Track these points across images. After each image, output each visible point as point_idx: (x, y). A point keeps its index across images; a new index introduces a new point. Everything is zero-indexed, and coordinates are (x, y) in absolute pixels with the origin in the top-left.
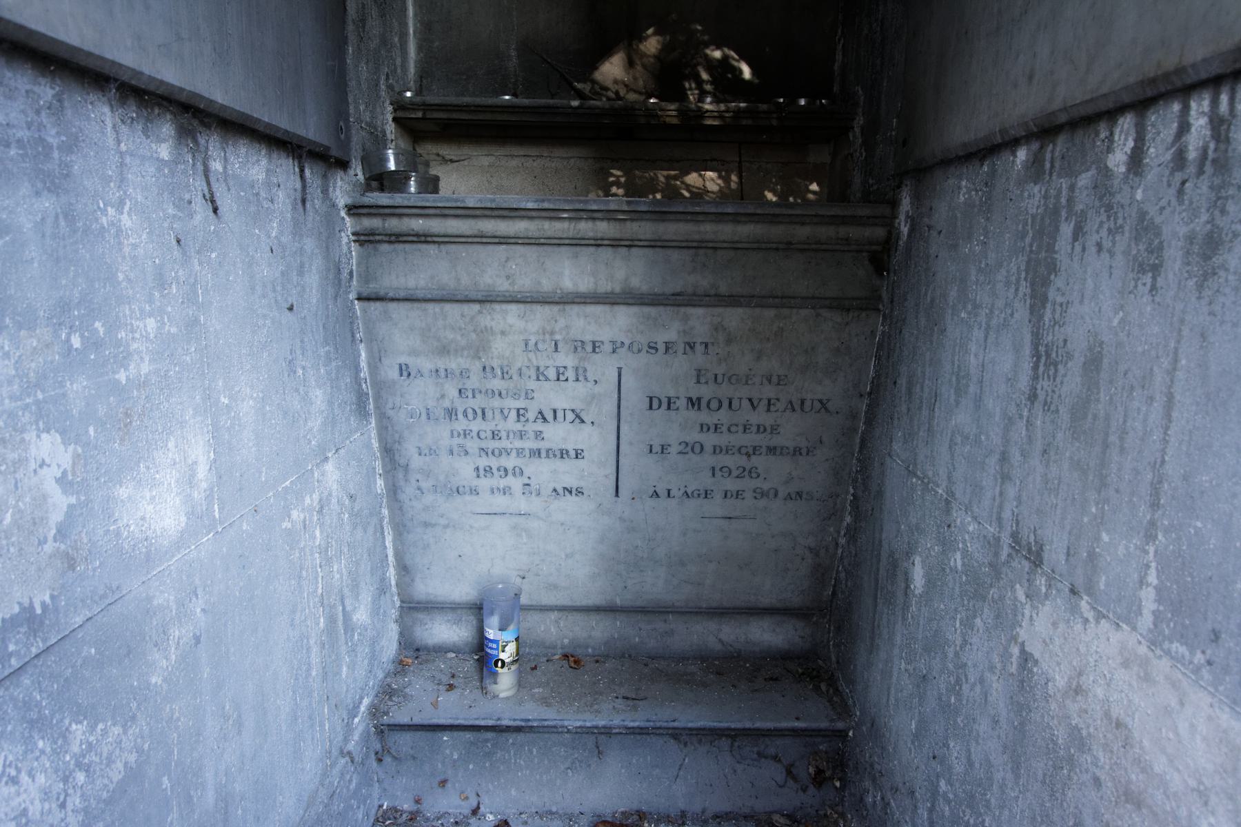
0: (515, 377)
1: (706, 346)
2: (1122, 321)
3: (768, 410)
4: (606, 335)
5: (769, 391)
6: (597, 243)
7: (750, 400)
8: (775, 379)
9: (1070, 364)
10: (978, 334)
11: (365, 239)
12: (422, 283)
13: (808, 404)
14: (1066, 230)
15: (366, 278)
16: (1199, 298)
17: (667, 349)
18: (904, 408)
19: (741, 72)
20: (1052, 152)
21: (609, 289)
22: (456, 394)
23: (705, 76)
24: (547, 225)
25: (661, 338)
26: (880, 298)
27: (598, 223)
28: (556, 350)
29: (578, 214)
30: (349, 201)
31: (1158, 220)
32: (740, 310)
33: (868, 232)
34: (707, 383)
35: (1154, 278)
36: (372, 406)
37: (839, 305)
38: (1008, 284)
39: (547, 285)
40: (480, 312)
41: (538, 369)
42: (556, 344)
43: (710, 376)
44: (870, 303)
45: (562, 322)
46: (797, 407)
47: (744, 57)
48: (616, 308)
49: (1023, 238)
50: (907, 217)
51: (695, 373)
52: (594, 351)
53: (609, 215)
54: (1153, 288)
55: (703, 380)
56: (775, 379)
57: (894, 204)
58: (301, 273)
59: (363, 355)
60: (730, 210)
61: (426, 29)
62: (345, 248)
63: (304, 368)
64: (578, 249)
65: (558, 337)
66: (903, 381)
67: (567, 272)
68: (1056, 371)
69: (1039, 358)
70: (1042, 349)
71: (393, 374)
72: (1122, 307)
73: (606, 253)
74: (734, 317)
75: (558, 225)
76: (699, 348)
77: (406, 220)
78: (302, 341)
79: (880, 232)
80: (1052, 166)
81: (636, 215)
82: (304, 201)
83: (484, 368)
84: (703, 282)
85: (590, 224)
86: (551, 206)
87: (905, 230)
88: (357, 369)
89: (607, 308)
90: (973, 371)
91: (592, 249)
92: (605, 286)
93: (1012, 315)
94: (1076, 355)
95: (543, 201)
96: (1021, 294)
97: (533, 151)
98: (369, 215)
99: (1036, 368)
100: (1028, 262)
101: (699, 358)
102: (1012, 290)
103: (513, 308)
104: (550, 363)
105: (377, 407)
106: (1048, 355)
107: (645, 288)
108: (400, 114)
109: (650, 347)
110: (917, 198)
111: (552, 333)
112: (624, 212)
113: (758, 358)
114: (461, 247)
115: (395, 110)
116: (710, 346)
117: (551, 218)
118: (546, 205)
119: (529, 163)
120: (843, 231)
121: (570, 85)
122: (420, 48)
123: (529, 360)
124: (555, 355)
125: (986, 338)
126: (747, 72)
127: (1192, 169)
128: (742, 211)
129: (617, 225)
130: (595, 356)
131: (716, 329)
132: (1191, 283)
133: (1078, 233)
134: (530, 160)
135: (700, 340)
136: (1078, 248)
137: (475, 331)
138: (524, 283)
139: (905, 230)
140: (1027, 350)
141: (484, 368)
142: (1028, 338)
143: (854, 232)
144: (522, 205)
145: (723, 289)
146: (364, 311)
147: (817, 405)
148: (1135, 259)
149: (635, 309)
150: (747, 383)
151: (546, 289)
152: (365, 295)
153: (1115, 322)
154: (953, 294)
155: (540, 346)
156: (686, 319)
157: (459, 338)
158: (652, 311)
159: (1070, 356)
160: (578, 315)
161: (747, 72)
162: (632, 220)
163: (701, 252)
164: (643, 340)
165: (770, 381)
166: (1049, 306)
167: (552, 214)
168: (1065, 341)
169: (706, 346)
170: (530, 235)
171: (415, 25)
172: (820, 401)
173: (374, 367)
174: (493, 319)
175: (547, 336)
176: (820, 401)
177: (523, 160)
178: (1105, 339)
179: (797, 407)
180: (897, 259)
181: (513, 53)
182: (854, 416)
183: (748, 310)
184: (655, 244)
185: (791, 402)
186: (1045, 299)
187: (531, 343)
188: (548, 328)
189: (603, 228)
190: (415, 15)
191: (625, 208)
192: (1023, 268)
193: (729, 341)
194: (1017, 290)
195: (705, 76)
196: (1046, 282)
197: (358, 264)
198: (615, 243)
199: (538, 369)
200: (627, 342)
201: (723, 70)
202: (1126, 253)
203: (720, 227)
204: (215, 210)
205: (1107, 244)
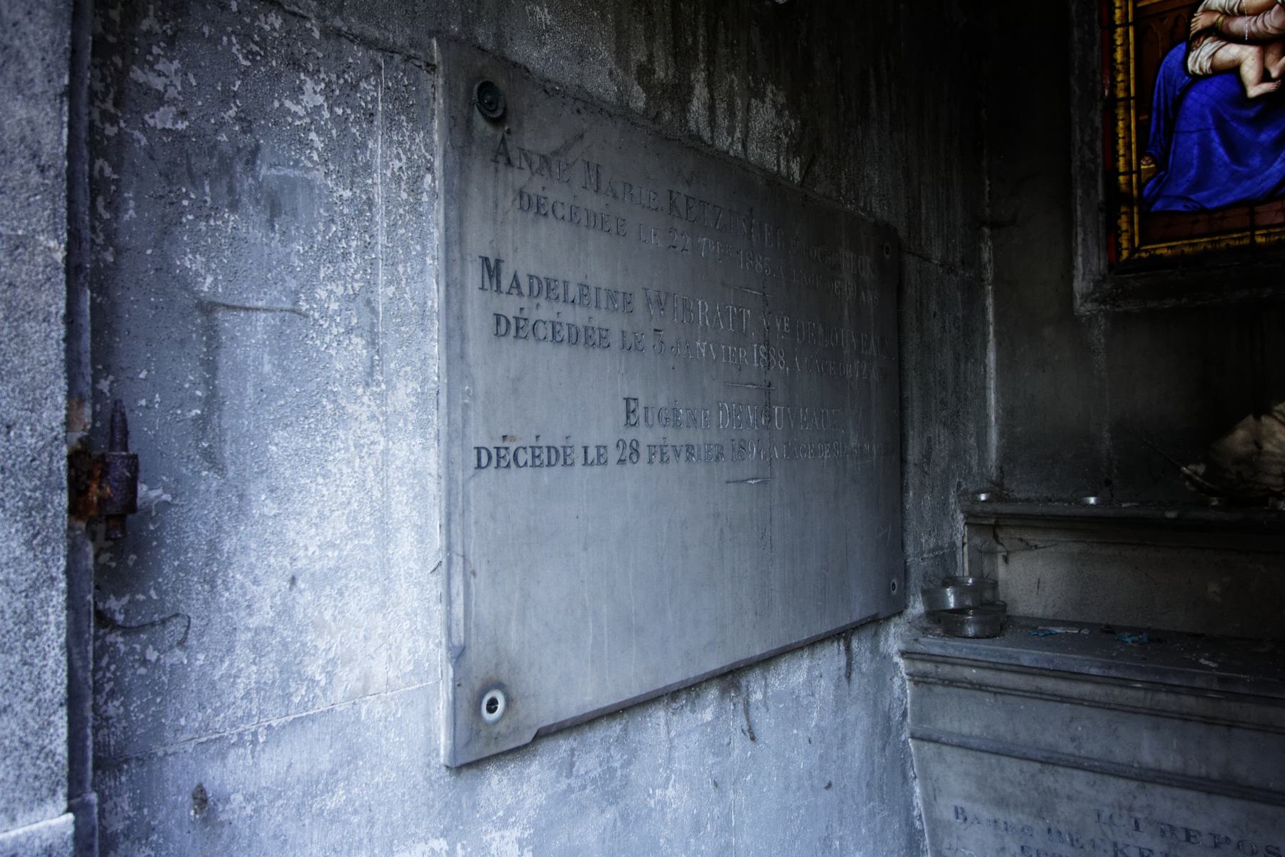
0: (1088, 848)
6: (1185, 717)
11: (920, 680)
12: (976, 731)
15: (920, 718)
21: (1203, 771)
22: (1018, 851)
24: (1117, 691)
28: (1137, 828)
29: (1153, 687)
30: (903, 647)
36: (927, 841)
39: (1120, 754)
40: (1042, 772)
41: (1115, 845)
42: (1136, 822)
45: (1141, 801)
58: (842, 745)
59: (918, 790)
61: (1009, 414)
62: (897, 691)
63: (841, 838)
65: (1138, 815)
71: (949, 815)
75: (1130, 693)
77: (959, 669)
78: (841, 812)
82: (848, 676)
83: (1049, 830)
85: (1172, 698)
88: (909, 807)
92: (1197, 768)
95: (1110, 668)
98: (922, 660)
104: (1130, 841)
105: (932, 844)
108: (971, 520)
114: (1019, 700)
115: (966, 518)
117: (1120, 686)
118: (1113, 673)
122: (1001, 435)
123: (1104, 834)
124: (1137, 834)
137: (1036, 789)
141: (1049, 830)
144: (1085, 670)
146: (917, 748)
152: (917, 735)
155: (1116, 820)
157: (1018, 793)
158: (1269, 810)
170: (1097, 698)
171: (997, 412)
173: (929, 805)
174: (1057, 781)
175: (1125, 812)
181: (1106, 435)
189: (1189, 702)
190: (997, 402)
191: (1216, 686)
197: (913, 703)
199: (1115, 845)
200: (1235, 839)
204: (753, 739)
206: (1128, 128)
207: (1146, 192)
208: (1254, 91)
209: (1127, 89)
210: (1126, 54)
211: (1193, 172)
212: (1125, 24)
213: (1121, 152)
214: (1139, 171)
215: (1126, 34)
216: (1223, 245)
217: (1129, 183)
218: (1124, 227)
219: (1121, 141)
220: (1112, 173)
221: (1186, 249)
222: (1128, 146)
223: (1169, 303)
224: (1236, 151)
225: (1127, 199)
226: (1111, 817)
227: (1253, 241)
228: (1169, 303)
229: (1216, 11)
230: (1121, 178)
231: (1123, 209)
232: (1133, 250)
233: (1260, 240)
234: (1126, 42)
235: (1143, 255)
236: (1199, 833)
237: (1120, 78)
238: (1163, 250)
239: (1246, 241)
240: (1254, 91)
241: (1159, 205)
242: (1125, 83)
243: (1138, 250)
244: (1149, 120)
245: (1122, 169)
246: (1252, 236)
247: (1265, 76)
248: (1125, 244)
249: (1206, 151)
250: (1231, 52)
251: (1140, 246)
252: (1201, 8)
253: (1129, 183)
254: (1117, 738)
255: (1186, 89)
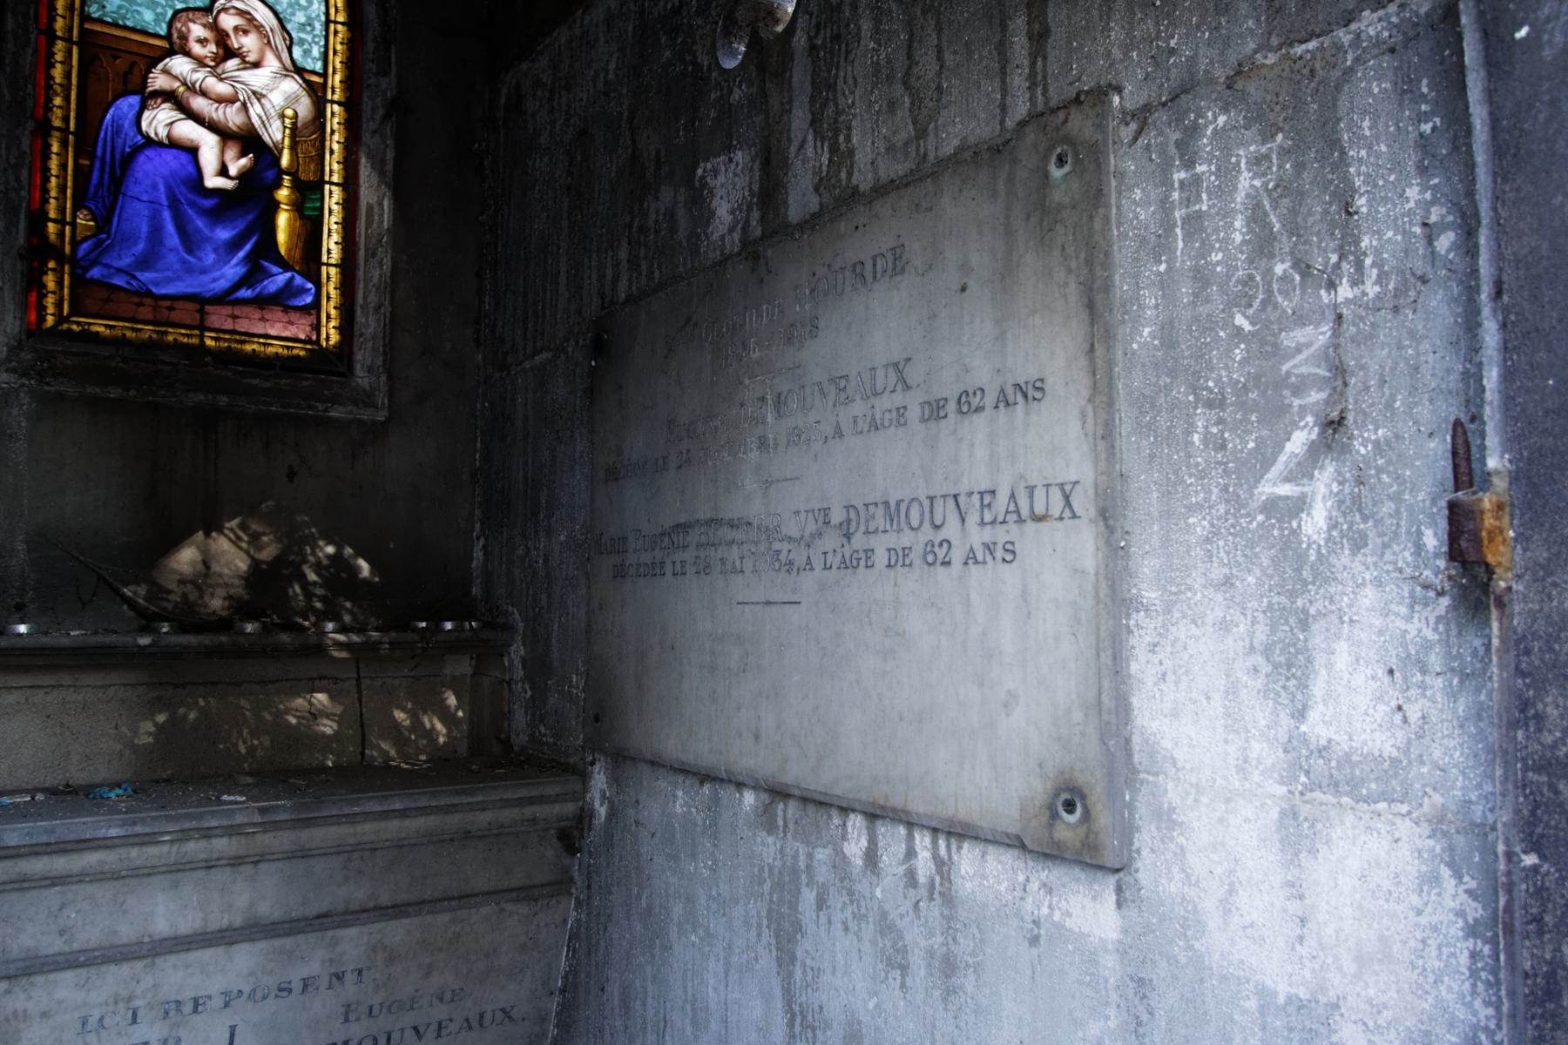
1: (360, 972)
2: (877, 1006)
3: (439, 1036)
4: (214, 986)
5: (441, 1012)
7: (415, 1028)
8: (448, 996)
9: (829, 1033)
10: (714, 967)
13: (488, 1017)
14: (808, 897)
16: (945, 1009)
17: (305, 987)
18: (619, 1023)
19: (358, 569)
20: (785, 811)
21: (225, 923)
23: (312, 577)
24: (134, 852)
25: (296, 976)
26: (571, 879)
27: (214, 841)
28: (134, 1020)
31: (900, 924)
32: (406, 921)
33: (556, 809)
34: (358, 1019)
35: (903, 976)
37: (527, 893)
38: (747, 924)
39: (127, 933)
42: (135, 1015)
43: (364, 1009)
44: (561, 885)
45: (148, 981)
46: (475, 1024)
47: (360, 553)
48: (235, 947)
49: (761, 882)
50: (603, 796)
51: (343, 1010)
52: (195, 1011)
53: (232, 831)
54: (903, 986)
55: (352, 1017)
56: (448, 996)
57: (584, 777)
60: (398, 806)
64: (179, 875)
65: (138, 1003)
66: (614, 990)
67: (161, 910)
68: (815, 1036)
69: (793, 1016)
70: (797, 1009)
72: (876, 994)
73: (222, 876)
74: (397, 931)
75: (153, 851)
76: (350, 978)
79: (570, 808)
80: (786, 826)
81: (266, 827)
84: (358, 894)
85: (203, 844)
86: (148, 830)
87: (602, 811)
89: (220, 950)
90: (713, 1007)
91: (201, 873)
92: (219, 920)
93: (756, 959)
94: (835, 1026)
95: (134, 823)
96: (764, 942)
97: (46, 680)
99: (791, 1024)
100: (769, 911)
101: (350, 989)
102: (754, 932)
103: (69, 975)
106: (804, 1018)
107: (277, 914)
109: (280, 990)
110: (615, 780)
111: (130, 999)
112: (254, 824)
113: (428, 974)
116: (365, 973)
118: (139, 829)
119: (39, 697)
120: (528, 811)
121: (117, 592)
125: (726, 975)
126: (364, 566)
127: (923, 892)
128: (413, 805)
129: (243, 840)
130: (197, 1018)
131: (374, 950)
132: (937, 993)
133: (821, 903)
134: (41, 693)
135: (352, 967)
136: (823, 920)
138: (91, 935)
139: (602, 811)
140: (779, 1004)
142: (778, 991)
143: (540, 811)
144: (101, 833)
145: (385, 899)
147: (500, 1015)
148: (883, 951)
149: (263, 945)
150: (412, 1008)
151: (125, 940)
153: (871, 1005)
154: (678, 910)
155: (107, 1022)
156: (335, 943)
158: (288, 942)
159: (828, 1026)
160: (175, 967)
161: (364, 566)
162: (265, 832)
163: (356, 855)
164: (272, 982)
165: (441, 999)
166: (798, 964)
168: (821, 1008)
169: (360, 972)
172: (503, 1011)
176: (503, 1011)
177: (28, 692)
178: (864, 1020)
179: (475, 1024)
180: (593, 838)
181: (20, 547)
182: (543, 1020)
183: (416, 920)
185: (467, 1020)
186: (793, 959)
187: (93, 1021)
188: (125, 994)
189: (221, 845)
191: (258, 819)
192: (764, 914)
193: (390, 960)
194: (759, 935)
195: (312, 577)
196: (792, 940)
198: (236, 862)
200: (247, 989)
201: (339, 575)
202: (874, 943)
203: (384, 824)
205: (853, 926)
206: (63, 166)
207: (81, 253)
208: (212, 181)
209: (66, 119)
210: (67, 75)
211: (141, 246)
212: (68, 39)
213: (53, 193)
214: (73, 224)
215: (69, 53)
216: (170, 338)
217: (61, 234)
218: (51, 285)
219: (53, 180)
220: (38, 219)
221: (129, 334)
222: (62, 189)
223: (114, 393)
224: (190, 241)
225: (55, 252)
226: (101, 1019)
227: (202, 342)
228: (114, 393)
229: (176, 78)
230: (52, 227)
231: (51, 265)
232: (60, 318)
233: (209, 342)
234: (67, 61)
235: (74, 327)
236: (210, 997)
237: (58, 101)
238: (99, 327)
239: (195, 341)
240: (212, 181)
241: (95, 273)
242: (62, 110)
243: (66, 320)
244: (91, 167)
245: (52, 215)
246: (202, 337)
247: (223, 171)
248: (51, 310)
249: (156, 230)
250: (188, 130)
251: (71, 314)
252: (160, 66)
253: (61, 234)
254: (125, 912)
255: (138, 149)
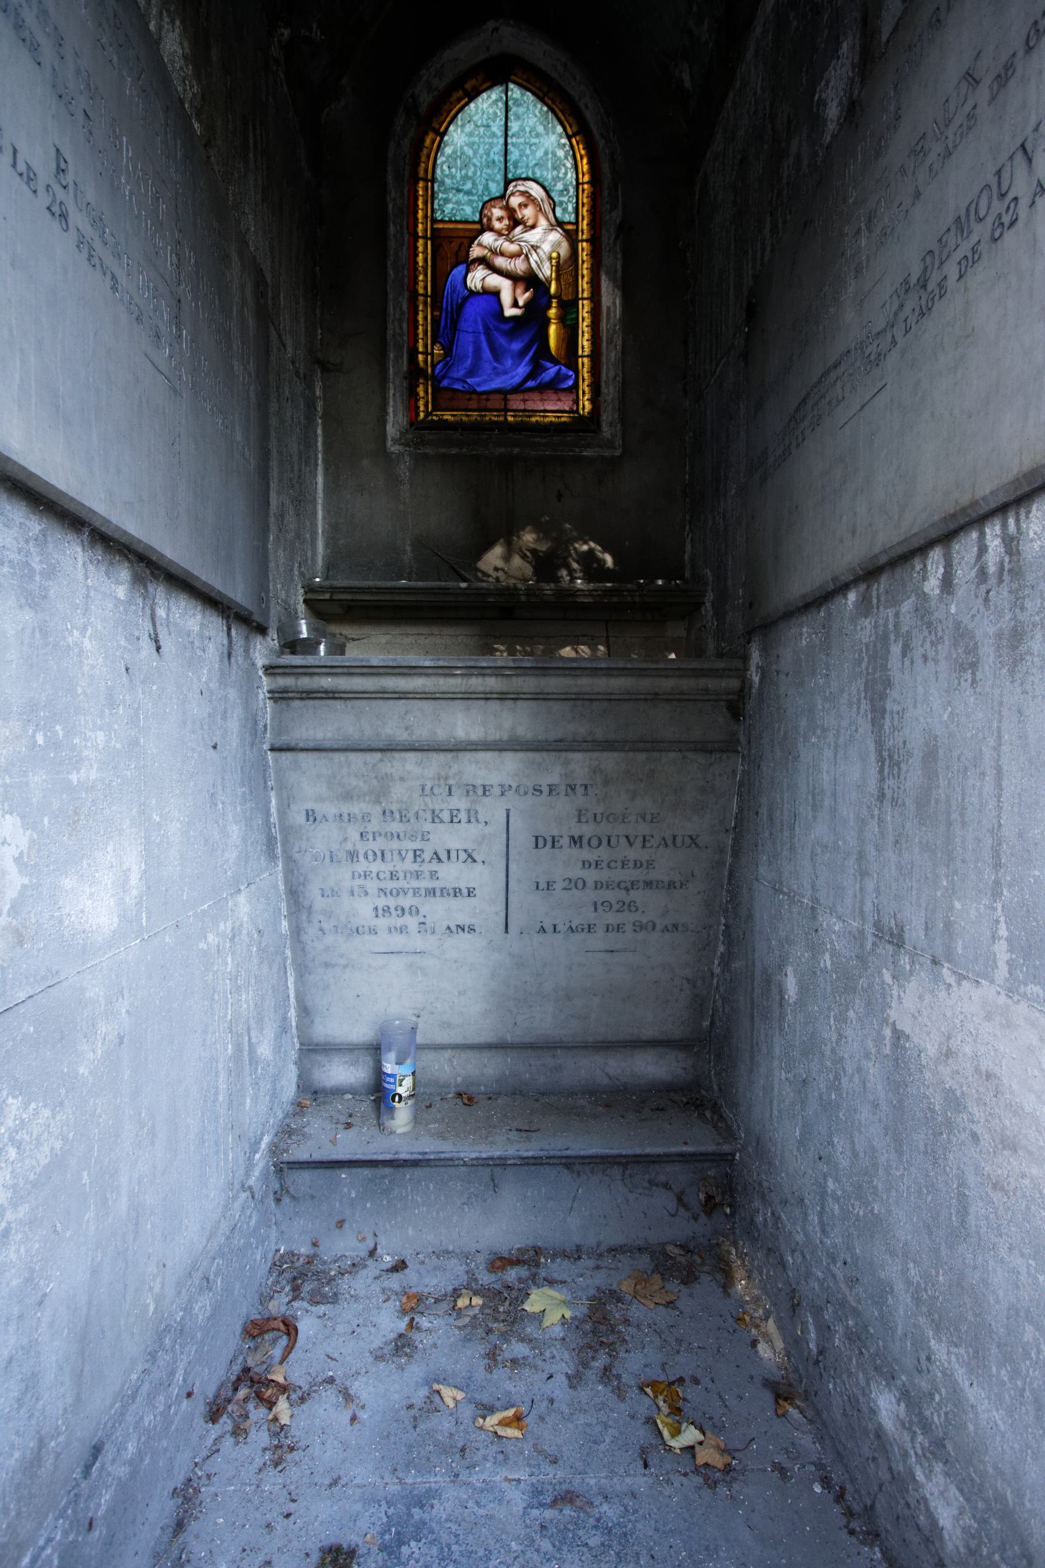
0: (413, 820)
3: (644, 846)
4: (494, 778)
5: (644, 829)
6: (487, 697)
7: (627, 837)
8: (648, 817)
9: (911, 761)
10: (828, 753)
11: (279, 696)
12: (329, 735)
13: (679, 840)
14: (896, 650)
15: (279, 731)
16: (1012, 682)
17: (551, 791)
18: (767, 834)
19: (605, 562)
20: (878, 590)
21: (498, 737)
22: (358, 837)
23: (575, 566)
24: (442, 681)
25: (545, 781)
26: (738, 741)
28: (450, 794)
29: (470, 671)
30: (267, 662)
31: (970, 626)
32: (615, 754)
34: (587, 822)
35: (973, 674)
36: (279, 851)
37: (703, 748)
39: (442, 735)
40: (382, 760)
41: (433, 812)
42: (450, 789)
43: (590, 815)
44: (729, 746)
46: (670, 843)
47: (605, 549)
49: (860, 664)
50: (758, 667)
51: (576, 813)
52: (484, 794)
53: (497, 671)
55: (583, 819)
56: (648, 817)
57: (745, 658)
58: (224, 718)
59: (273, 802)
61: (333, 529)
62: (261, 703)
63: (223, 803)
64: (470, 702)
65: (451, 782)
66: (764, 811)
67: (460, 723)
68: (899, 769)
69: (883, 763)
70: (885, 754)
71: (301, 819)
72: (949, 703)
73: (495, 705)
74: (610, 761)
75: (452, 681)
76: (580, 790)
77: (316, 679)
78: (223, 779)
79: (734, 684)
80: (879, 600)
82: (229, 655)
83: (384, 812)
84: (581, 729)
85: (480, 680)
86: (446, 664)
87: (756, 679)
88: (268, 814)
89: (496, 754)
91: (482, 702)
92: (493, 735)
93: (856, 731)
94: (915, 752)
95: (439, 660)
96: (862, 711)
97: (425, 630)
98: (284, 674)
99: (881, 771)
100: (866, 684)
101: (580, 799)
102: (855, 709)
103: (411, 755)
104: (443, 806)
105: (284, 851)
107: (529, 736)
108: (310, 596)
109: (535, 790)
110: (765, 650)
111: (446, 778)
113: (633, 798)
114: (364, 702)
115: (306, 593)
116: (589, 787)
117: (445, 675)
118: (441, 663)
119: (422, 640)
120: (703, 682)
122: (327, 546)
123: (426, 804)
124: (449, 799)
125: (835, 755)
126: (609, 560)
127: (993, 581)
128: (614, 666)
130: (486, 800)
131: (595, 772)
132: (1004, 671)
133: (906, 650)
134: (423, 637)
136: (907, 662)
137: (376, 777)
138: (422, 733)
139: (756, 679)
140: (873, 758)
141: (384, 812)
142: (872, 747)
143: (712, 683)
144: (421, 664)
146: (276, 761)
147: (688, 841)
148: (956, 660)
149: (521, 755)
150: (623, 822)
151: (441, 738)
152: (277, 746)
154: (803, 723)
155: (436, 791)
157: (361, 784)
158: (537, 756)
159: (910, 755)
161: (609, 560)
162: (517, 675)
163: (579, 703)
164: (530, 783)
165: (644, 820)
166: (887, 716)
167: (446, 671)
168: (905, 743)
169: (586, 787)
170: (427, 690)
171: (323, 526)
172: (691, 837)
173: (282, 813)
174: (392, 767)
175: (442, 781)
176: (691, 837)
178: (938, 733)
179: (670, 843)
180: (751, 705)
181: (408, 548)
182: (722, 851)
183: (622, 754)
184: (538, 697)
185: (664, 839)
186: (884, 711)
187: (428, 788)
188: (443, 774)
189: (492, 683)
190: (324, 518)
191: (511, 664)
192: (862, 689)
193: (607, 782)
194: (859, 708)
195: (575, 566)
196: (883, 697)
197: (272, 719)
198: (502, 697)
199: (433, 812)
200: (514, 785)
201: (589, 560)
202: (948, 658)
204: (158, 649)
205: (931, 654)
206: (425, 318)
207: (437, 371)
208: (509, 312)
209: (426, 288)
210: (425, 260)
211: (469, 362)
212: (425, 237)
213: (421, 336)
214: (432, 354)
215: (426, 245)
216: (487, 418)
217: (426, 361)
218: (422, 394)
219: (420, 327)
220: (413, 353)
221: (464, 418)
222: (425, 332)
223: (454, 451)
224: (497, 354)
225: (422, 373)
226: (432, 789)
227: (506, 419)
228: (454, 451)
229: (485, 247)
230: (421, 357)
231: (421, 381)
232: (428, 414)
233: (510, 419)
234: (425, 252)
235: (435, 418)
236: (492, 786)
237: (421, 278)
238: (448, 416)
239: (502, 419)
240: (509, 312)
241: (445, 383)
242: (424, 283)
243: (431, 414)
244: (440, 315)
245: (421, 349)
246: (506, 416)
247: (515, 304)
248: (422, 408)
249: (477, 350)
250: (495, 281)
251: (433, 411)
252: (476, 242)
253: (426, 361)
254: (440, 722)
255: (465, 299)
